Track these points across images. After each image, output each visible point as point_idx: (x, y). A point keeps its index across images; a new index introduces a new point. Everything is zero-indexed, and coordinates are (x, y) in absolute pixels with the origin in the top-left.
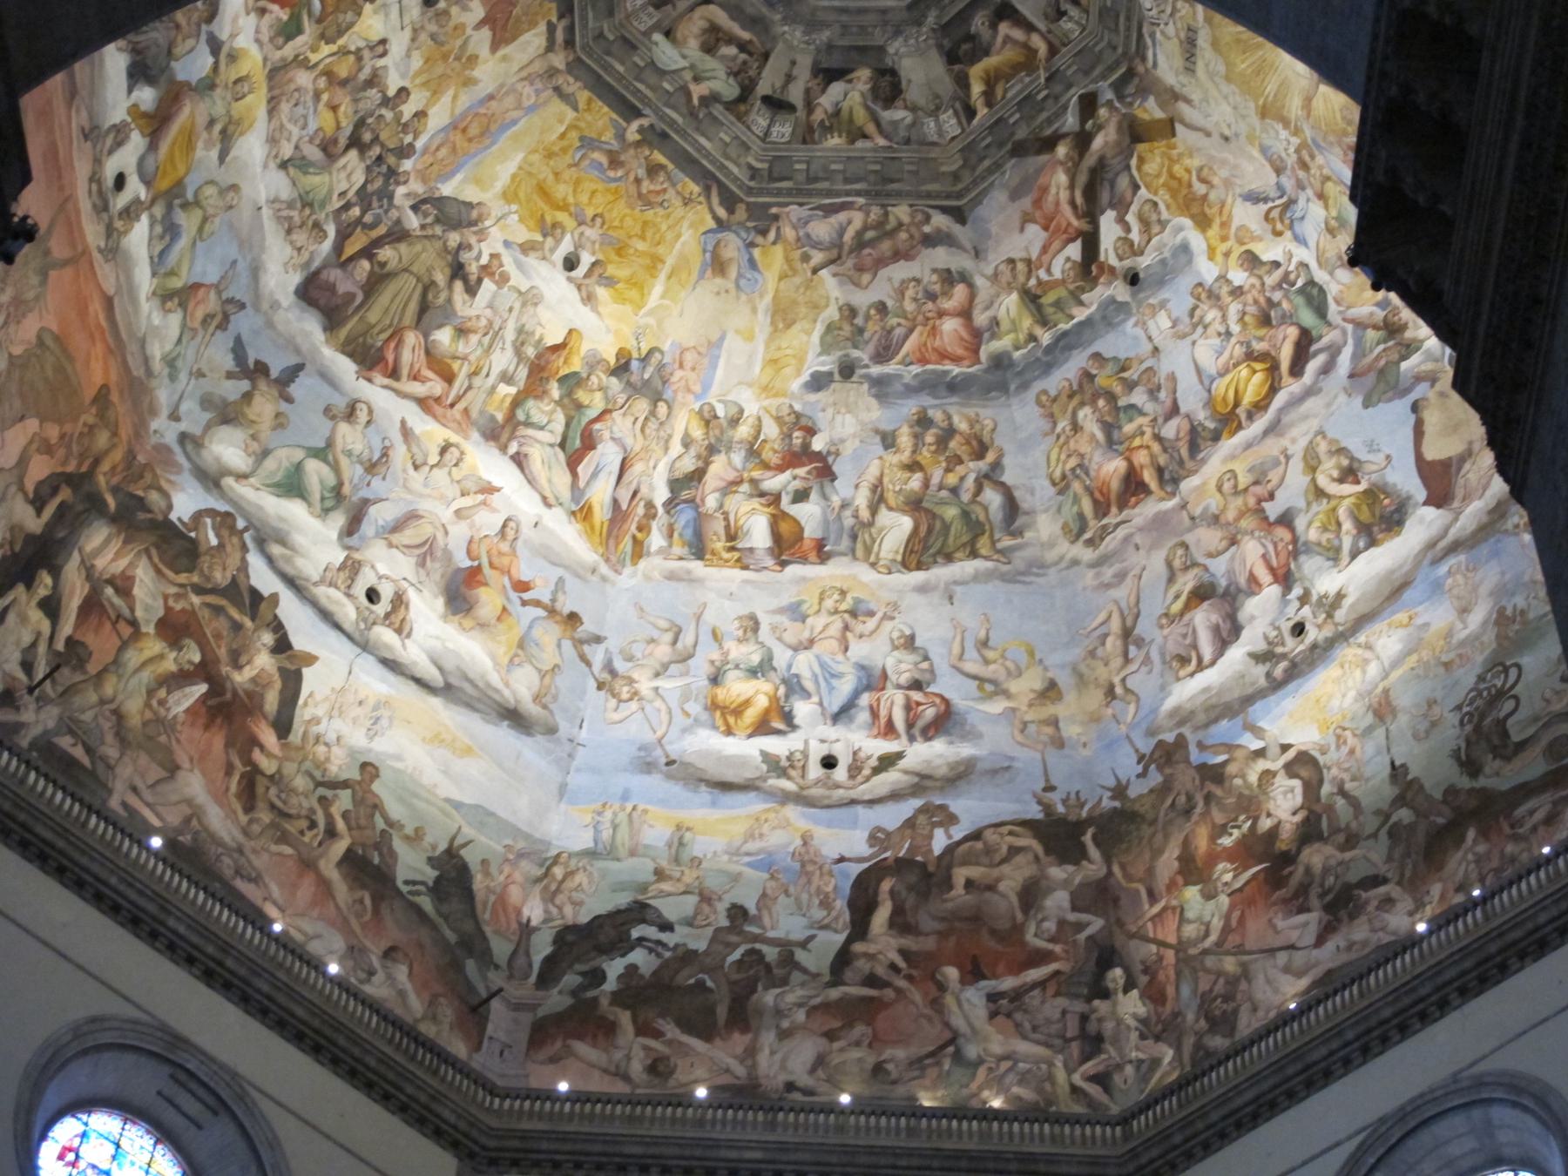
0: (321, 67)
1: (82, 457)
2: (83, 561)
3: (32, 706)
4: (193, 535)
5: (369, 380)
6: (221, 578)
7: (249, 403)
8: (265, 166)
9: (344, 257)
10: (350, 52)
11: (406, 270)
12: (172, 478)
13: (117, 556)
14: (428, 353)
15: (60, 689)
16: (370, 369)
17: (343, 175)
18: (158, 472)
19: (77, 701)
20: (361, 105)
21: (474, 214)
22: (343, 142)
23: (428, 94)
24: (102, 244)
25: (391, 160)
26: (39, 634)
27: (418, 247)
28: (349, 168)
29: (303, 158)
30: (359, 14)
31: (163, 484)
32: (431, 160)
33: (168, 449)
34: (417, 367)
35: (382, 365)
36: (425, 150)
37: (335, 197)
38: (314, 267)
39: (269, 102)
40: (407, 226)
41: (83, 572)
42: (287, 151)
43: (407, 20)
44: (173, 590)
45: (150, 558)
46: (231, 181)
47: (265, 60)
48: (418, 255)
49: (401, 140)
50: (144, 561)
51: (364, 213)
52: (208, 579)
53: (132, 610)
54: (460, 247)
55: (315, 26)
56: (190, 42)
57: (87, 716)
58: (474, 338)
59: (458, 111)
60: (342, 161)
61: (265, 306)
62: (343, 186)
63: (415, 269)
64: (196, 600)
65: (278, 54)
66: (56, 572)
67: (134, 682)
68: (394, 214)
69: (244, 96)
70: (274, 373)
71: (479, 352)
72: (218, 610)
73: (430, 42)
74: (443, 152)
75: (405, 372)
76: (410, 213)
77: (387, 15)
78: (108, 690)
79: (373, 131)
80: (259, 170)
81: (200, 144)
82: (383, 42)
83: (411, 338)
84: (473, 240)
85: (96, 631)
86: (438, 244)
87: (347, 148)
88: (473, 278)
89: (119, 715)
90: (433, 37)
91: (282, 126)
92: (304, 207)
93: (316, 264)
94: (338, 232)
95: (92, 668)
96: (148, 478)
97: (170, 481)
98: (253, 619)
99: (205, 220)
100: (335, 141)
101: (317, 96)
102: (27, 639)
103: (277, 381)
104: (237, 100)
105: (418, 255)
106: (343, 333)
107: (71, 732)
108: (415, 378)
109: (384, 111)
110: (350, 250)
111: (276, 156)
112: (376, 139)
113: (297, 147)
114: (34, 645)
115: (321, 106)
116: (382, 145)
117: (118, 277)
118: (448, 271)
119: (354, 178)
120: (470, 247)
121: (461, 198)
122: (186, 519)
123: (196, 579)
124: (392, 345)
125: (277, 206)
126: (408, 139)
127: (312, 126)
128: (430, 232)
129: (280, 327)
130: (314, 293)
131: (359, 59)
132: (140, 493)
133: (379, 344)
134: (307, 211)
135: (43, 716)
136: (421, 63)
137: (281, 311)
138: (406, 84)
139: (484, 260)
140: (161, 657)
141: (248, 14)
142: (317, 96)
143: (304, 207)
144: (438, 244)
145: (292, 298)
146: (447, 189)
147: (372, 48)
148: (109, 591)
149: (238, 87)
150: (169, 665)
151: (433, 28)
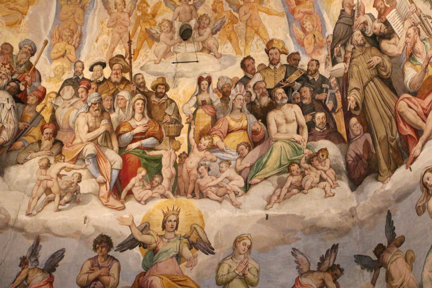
0: (193, 142)
5: (415, 158)
7: (393, 279)
8: (238, 206)
9: (345, 137)
10: (195, 113)
11: (364, 88)
14: (415, 94)
16: (409, 154)
17: (284, 128)
20: (238, 106)
21: (348, 11)
22: (258, 126)
23: (256, 37)
25: (294, 77)
27: (355, 69)
28: (281, 120)
29: (251, 167)
30: (172, 101)
32: (310, 36)
34: (420, 110)
35: (410, 143)
36: (300, 43)
37: (298, 137)
38: (343, 166)
39: (194, 196)
40: (341, 74)
42: (239, 182)
43: (193, 57)
46: (230, 244)
47: (163, 196)
48: (359, 72)
49: (282, 66)
51: (325, 108)
54: (363, 32)
55: (163, 145)
56: (114, 270)
58: (419, 46)
59: (280, 9)
60: (273, 128)
61: (348, 223)
62: (293, 127)
63: (366, 80)
65: (165, 183)
68: (333, 81)
69: (177, 221)
70: (385, 243)
71: (428, 44)
73: (216, 36)
74: (308, 25)
75: (420, 123)
76: (336, 67)
77: (182, 76)
79: (263, 95)
80: (238, 213)
81: (187, 272)
82: (200, 80)
83: (402, 106)
84: (362, 19)
86: (358, 52)
87: (265, 122)
88: (384, 29)
90: (213, 33)
91: (218, 186)
92: (289, 171)
93: (342, 163)
94: (326, 138)
99: (243, 278)
100: (255, 132)
101: (213, 148)
103: (389, 244)
104: (177, 228)
105: (359, 72)
106: (383, 165)
108: (426, 115)
109: (252, 83)
110: (343, 131)
111: (236, 194)
112: (270, 92)
113: (240, 173)
115: (221, 145)
116: (278, 86)
118: (374, 50)
119: (291, 117)
120: (365, 23)
121: (337, 19)
124: (402, 124)
125: (275, 198)
126: (284, 59)
127: (232, 155)
128: (349, 55)
129: (365, 217)
130: (356, 175)
131: (204, 103)
133: (398, 136)
134: (295, 167)
136: (229, 45)
137: (358, 210)
138: (240, 59)
139: (375, 13)
141: (124, 208)
142: (213, 148)
143: (289, 171)
144: (358, 52)
145: (353, 194)
146: (330, 30)
147: (201, 91)
149: (169, 224)
151: (208, 30)
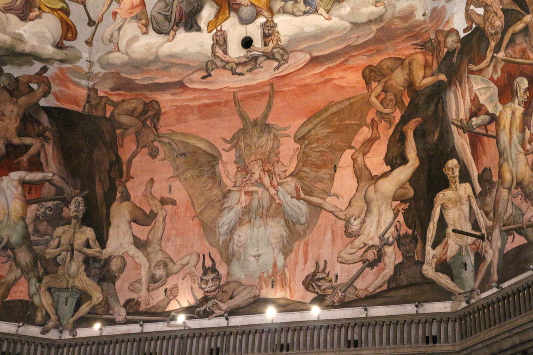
1: (398, 103)
2: (457, 126)
3: (488, 248)
4: (474, 26)
6: (499, 23)
12: (446, 19)
13: (463, 98)
15: (492, 215)
18: (440, 28)
19: (501, 208)
24: (276, 64)
26: (469, 197)
31: (447, 29)
33: (434, 10)
41: (461, 131)
44: (491, 69)
45: (471, 72)
50: (472, 77)
52: (496, 33)
53: (487, 113)
57: (510, 211)
64: (501, 55)
66: (453, 153)
67: (514, 151)
72: (512, 41)
78: (508, 176)
85: (484, 153)
89: (519, 184)
95: (495, 179)
96: (441, 38)
97: (447, 22)
98: (528, 13)
102: (466, 208)
107: (509, 232)
114: (471, 208)
117: (301, 51)
122: (465, 26)
123: (493, 44)
132: (446, 50)
135: (494, 247)
140: (513, 113)
148: (475, 121)
150: (520, 110)
